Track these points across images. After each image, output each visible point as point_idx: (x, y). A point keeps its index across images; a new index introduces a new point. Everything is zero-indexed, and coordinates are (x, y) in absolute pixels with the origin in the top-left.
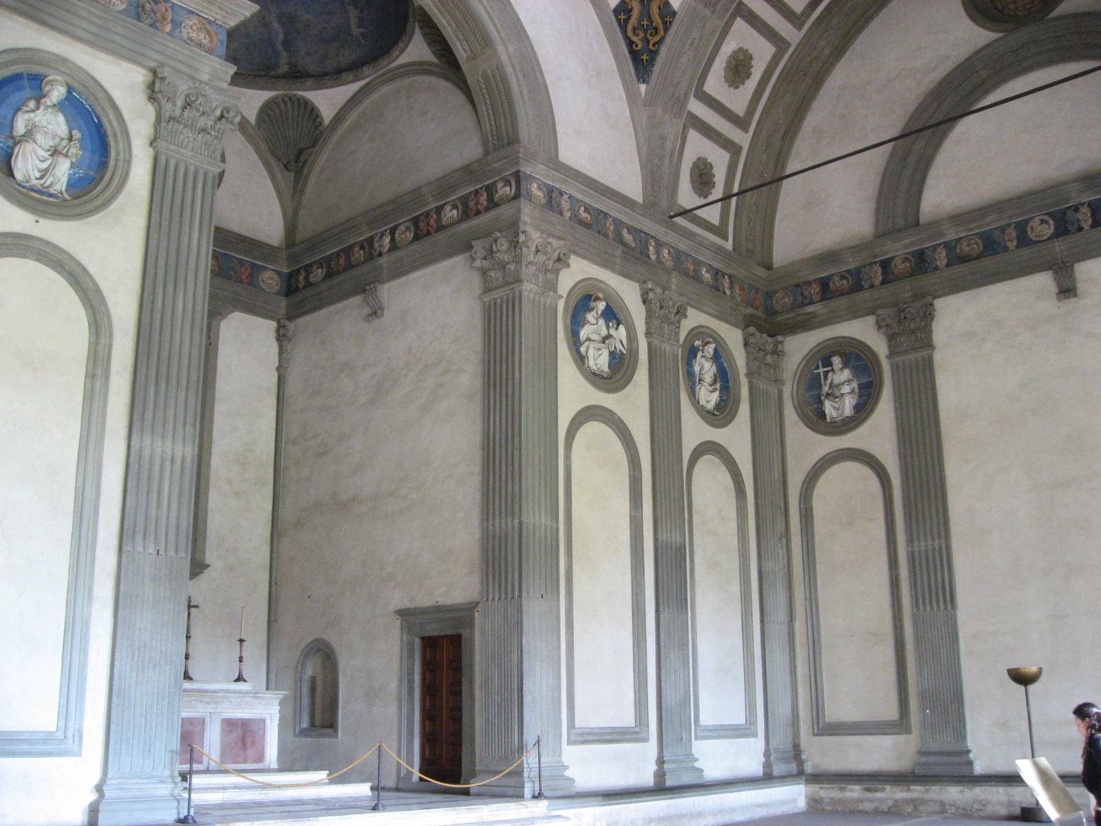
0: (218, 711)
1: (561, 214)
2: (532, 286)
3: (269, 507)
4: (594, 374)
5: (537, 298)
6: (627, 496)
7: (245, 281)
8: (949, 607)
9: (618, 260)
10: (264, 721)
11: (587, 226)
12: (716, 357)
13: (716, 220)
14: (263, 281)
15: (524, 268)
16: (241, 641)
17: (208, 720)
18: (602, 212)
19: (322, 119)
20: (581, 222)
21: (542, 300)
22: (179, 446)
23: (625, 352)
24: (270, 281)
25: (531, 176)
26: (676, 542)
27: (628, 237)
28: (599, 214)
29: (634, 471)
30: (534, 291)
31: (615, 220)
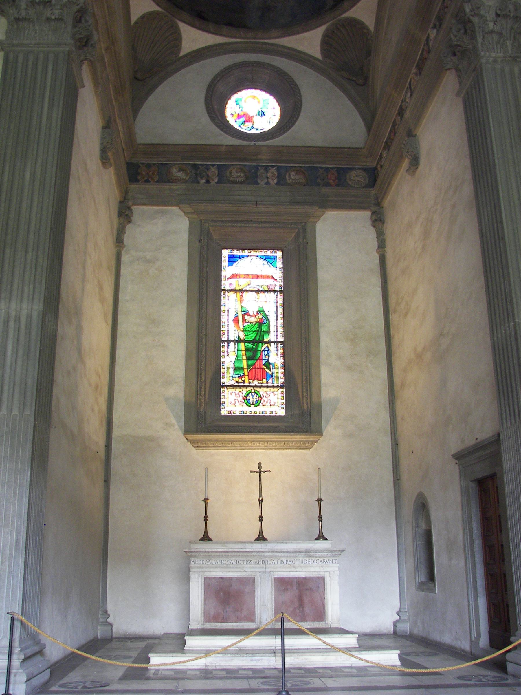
0: (267, 570)
2: (493, 55)
3: (384, 374)
5: (507, 69)
7: (333, 184)
10: (324, 579)
14: (350, 179)
15: (480, 40)
16: (320, 501)
17: (258, 579)
19: (368, 29)
22: (25, 305)
24: (358, 179)
30: (499, 60)
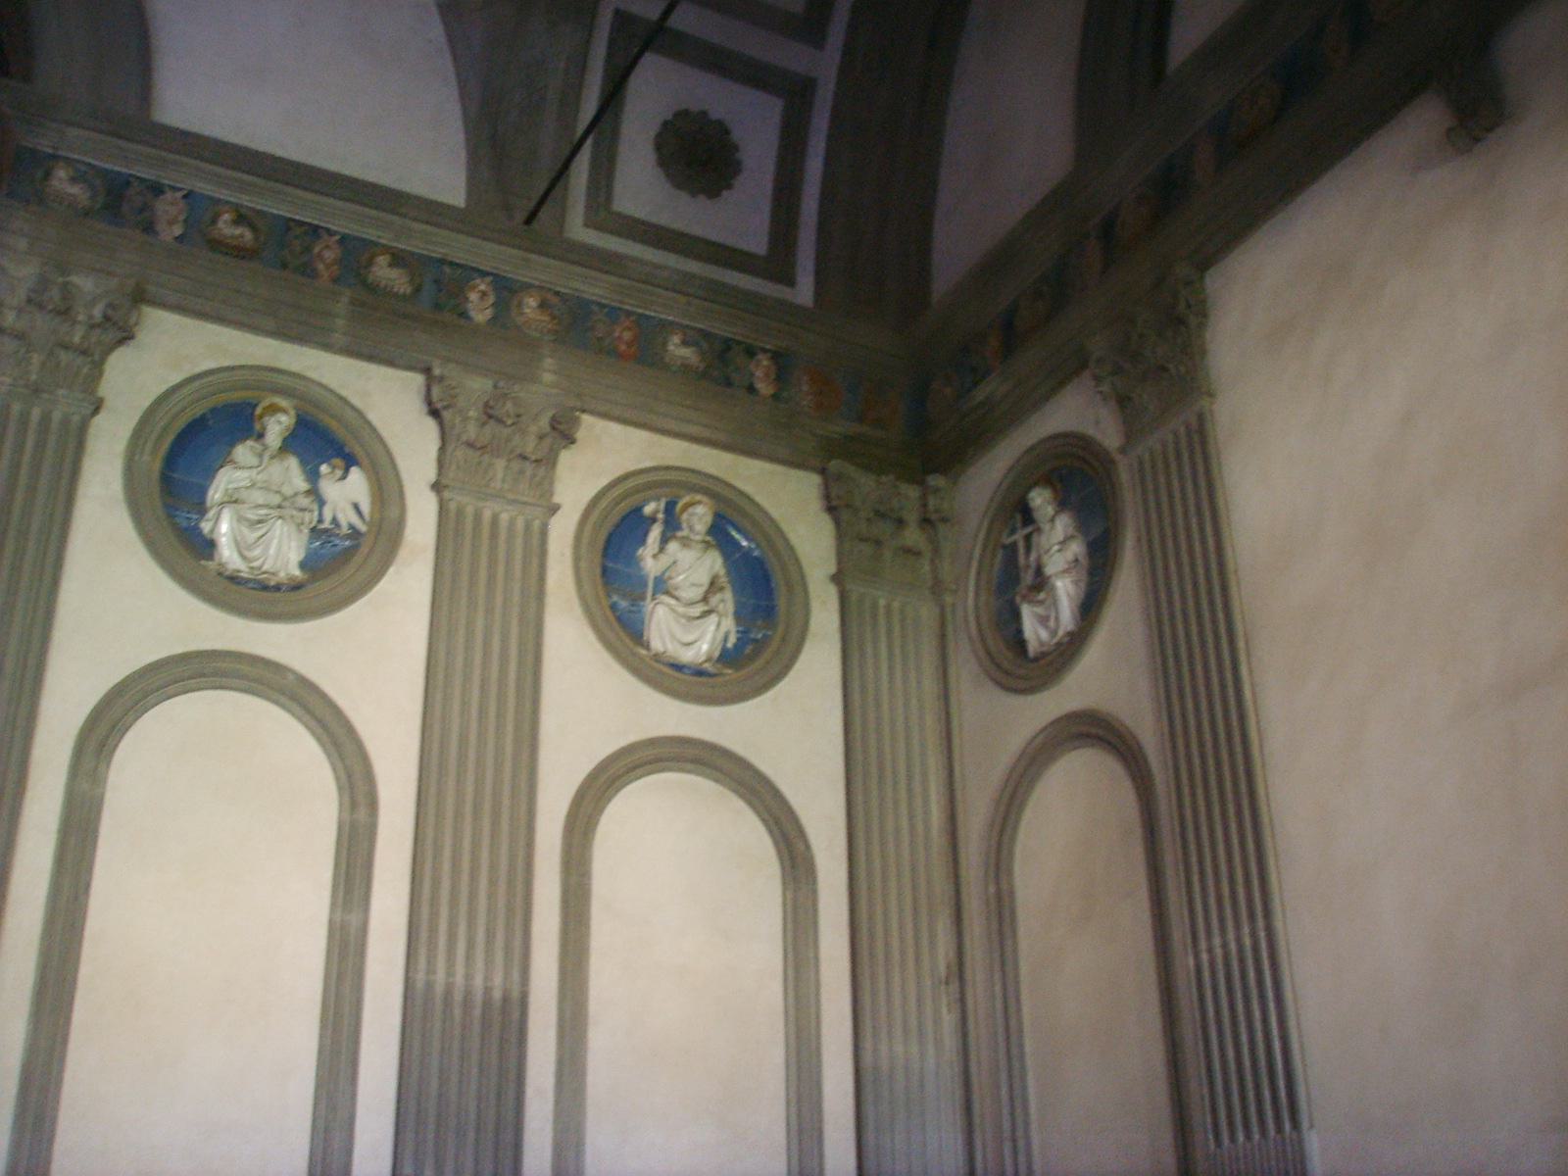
1: (149, 228)
4: (234, 579)
6: (327, 875)
8: (1287, 1126)
9: (340, 322)
11: (240, 252)
12: (719, 534)
13: (756, 242)
18: (301, 224)
20: (217, 245)
21: (36, 413)
23: (363, 528)
25: (55, 157)
26: (488, 990)
27: (384, 272)
28: (289, 229)
29: (354, 805)
31: (344, 240)
